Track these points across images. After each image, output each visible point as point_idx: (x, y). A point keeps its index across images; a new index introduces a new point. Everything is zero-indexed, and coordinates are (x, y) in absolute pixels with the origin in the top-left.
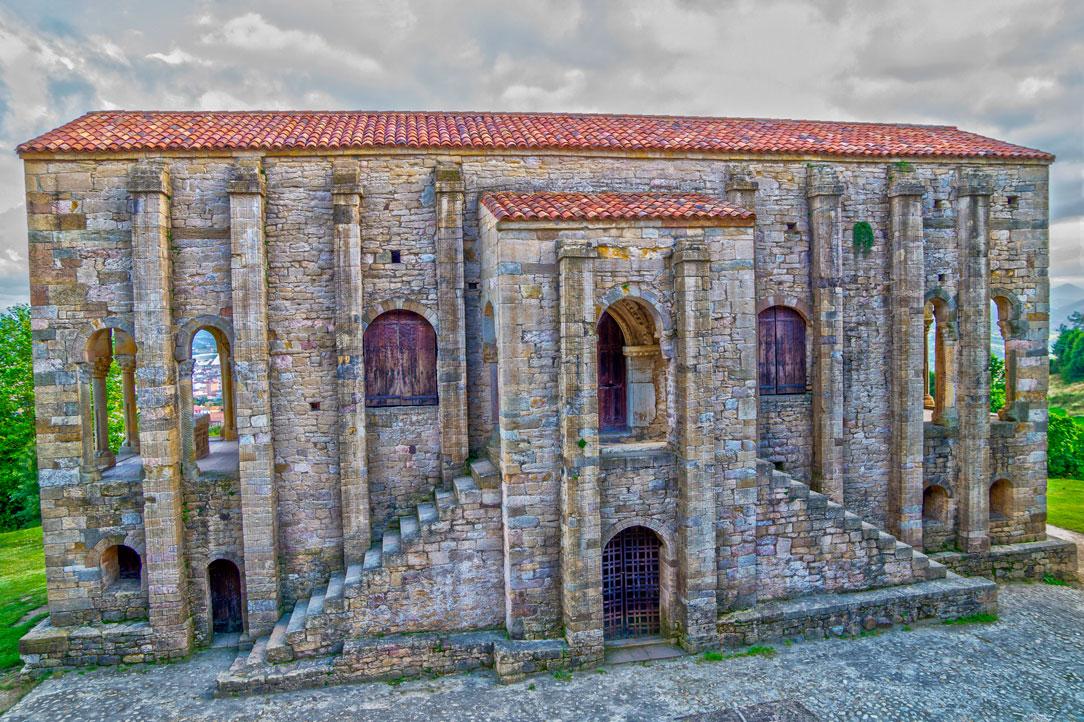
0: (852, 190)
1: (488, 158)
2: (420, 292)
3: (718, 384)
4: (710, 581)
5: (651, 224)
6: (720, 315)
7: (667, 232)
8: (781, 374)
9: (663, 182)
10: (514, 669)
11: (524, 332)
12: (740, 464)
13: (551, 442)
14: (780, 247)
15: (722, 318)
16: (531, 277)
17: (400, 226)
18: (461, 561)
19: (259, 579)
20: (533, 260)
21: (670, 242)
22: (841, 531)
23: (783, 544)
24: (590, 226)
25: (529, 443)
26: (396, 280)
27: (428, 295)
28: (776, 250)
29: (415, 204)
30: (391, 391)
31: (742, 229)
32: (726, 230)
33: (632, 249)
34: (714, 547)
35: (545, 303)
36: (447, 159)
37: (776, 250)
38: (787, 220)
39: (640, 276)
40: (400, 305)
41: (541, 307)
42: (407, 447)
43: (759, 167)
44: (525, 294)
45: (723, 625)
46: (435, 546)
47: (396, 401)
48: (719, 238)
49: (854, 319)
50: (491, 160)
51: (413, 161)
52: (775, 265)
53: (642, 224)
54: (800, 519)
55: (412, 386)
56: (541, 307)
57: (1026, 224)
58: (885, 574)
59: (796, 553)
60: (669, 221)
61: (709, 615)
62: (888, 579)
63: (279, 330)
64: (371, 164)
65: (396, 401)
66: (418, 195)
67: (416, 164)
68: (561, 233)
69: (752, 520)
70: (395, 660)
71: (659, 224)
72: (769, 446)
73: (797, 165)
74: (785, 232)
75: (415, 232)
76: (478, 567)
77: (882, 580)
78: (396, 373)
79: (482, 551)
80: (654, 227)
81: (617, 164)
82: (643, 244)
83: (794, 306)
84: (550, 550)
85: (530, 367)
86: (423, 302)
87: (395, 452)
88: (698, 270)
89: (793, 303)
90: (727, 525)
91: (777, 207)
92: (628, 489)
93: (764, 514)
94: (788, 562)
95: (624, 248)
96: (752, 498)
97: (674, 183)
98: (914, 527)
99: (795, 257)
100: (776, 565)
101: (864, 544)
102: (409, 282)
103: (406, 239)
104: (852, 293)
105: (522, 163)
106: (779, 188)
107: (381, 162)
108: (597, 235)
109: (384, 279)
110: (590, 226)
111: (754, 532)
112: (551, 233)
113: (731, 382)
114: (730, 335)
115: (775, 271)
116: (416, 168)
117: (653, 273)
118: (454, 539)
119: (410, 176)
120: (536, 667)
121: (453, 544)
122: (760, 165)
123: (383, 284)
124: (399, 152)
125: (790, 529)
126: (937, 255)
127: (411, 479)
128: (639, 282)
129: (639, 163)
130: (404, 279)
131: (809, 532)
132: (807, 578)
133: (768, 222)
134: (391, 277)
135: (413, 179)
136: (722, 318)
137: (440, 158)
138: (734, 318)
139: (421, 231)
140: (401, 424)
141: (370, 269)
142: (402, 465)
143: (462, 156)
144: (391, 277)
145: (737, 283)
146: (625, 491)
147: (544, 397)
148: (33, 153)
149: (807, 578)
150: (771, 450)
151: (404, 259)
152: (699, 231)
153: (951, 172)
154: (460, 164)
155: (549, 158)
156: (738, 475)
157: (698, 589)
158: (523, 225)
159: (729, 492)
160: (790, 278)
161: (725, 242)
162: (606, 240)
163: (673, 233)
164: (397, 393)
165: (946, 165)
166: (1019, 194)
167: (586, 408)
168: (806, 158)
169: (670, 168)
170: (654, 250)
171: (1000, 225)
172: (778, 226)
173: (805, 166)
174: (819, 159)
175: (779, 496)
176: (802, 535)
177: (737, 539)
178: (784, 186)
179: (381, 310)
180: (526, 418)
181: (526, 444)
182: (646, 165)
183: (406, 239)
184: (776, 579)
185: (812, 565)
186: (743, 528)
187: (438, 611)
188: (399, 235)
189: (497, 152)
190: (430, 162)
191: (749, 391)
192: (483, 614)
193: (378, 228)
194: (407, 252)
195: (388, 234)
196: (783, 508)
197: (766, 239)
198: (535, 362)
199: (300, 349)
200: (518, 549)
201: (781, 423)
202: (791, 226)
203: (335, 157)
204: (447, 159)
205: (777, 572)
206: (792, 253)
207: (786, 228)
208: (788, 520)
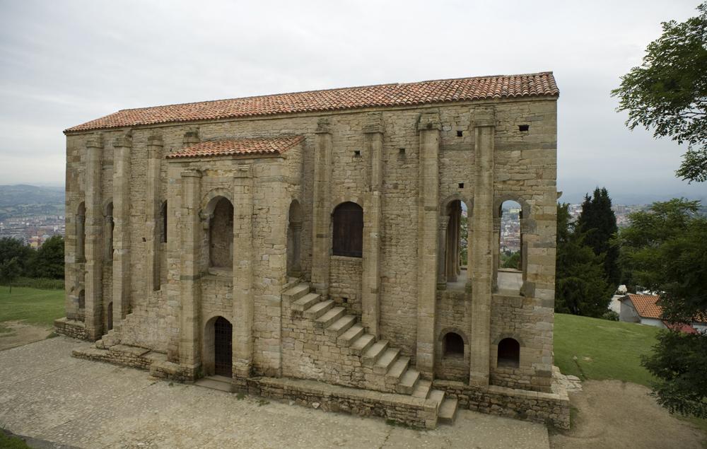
0: (396, 128)
6: (260, 208)
7: (235, 162)
9: (287, 131)
14: (350, 166)
15: (261, 209)
18: (161, 318)
19: (117, 311)
22: (335, 345)
23: (299, 345)
36: (193, 127)
43: (339, 118)
48: (261, 164)
49: (395, 212)
57: (535, 146)
58: (365, 380)
62: (366, 384)
63: (133, 205)
64: (167, 131)
68: (191, 164)
70: (126, 358)
71: (231, 158)
77: (363, 384)
81: (264, 123)
82: (224, 168)
88: (241, 182)
95: (216, 171)
97: (291, 131)
98: (426, 358)
101: (351, 357)
104: (394, 195)
106: (350, 130)
107: (170, 130)
108: (204, 165)
110: (202, 160)
120: (165, 376)
125: (302, 336)
126: (458, 170)
128: (222, 189)
129: (275, 121)
132: (314, 370)
136: (261, 209)
148: (67, 132)
149: (314, 370)
153: (472, 111)
154: (198, 128)
155: (234, 123)
162: (208, 167)
163: (239, 162)
165: (465, 106)
166: (528, 123)
169: (290, 123)
170: (230, 171)
171: (511, 147)
172: (348, 153)
174: (375, 110)
176: (309, 342)
182: (279, 122)
185: (316, 362)
191: (276, 251)
199: (139, 214)
202: (357, 153)
203: (155, 128)
204: (193, 127)
206: (356, 170)
207: (354, 153)
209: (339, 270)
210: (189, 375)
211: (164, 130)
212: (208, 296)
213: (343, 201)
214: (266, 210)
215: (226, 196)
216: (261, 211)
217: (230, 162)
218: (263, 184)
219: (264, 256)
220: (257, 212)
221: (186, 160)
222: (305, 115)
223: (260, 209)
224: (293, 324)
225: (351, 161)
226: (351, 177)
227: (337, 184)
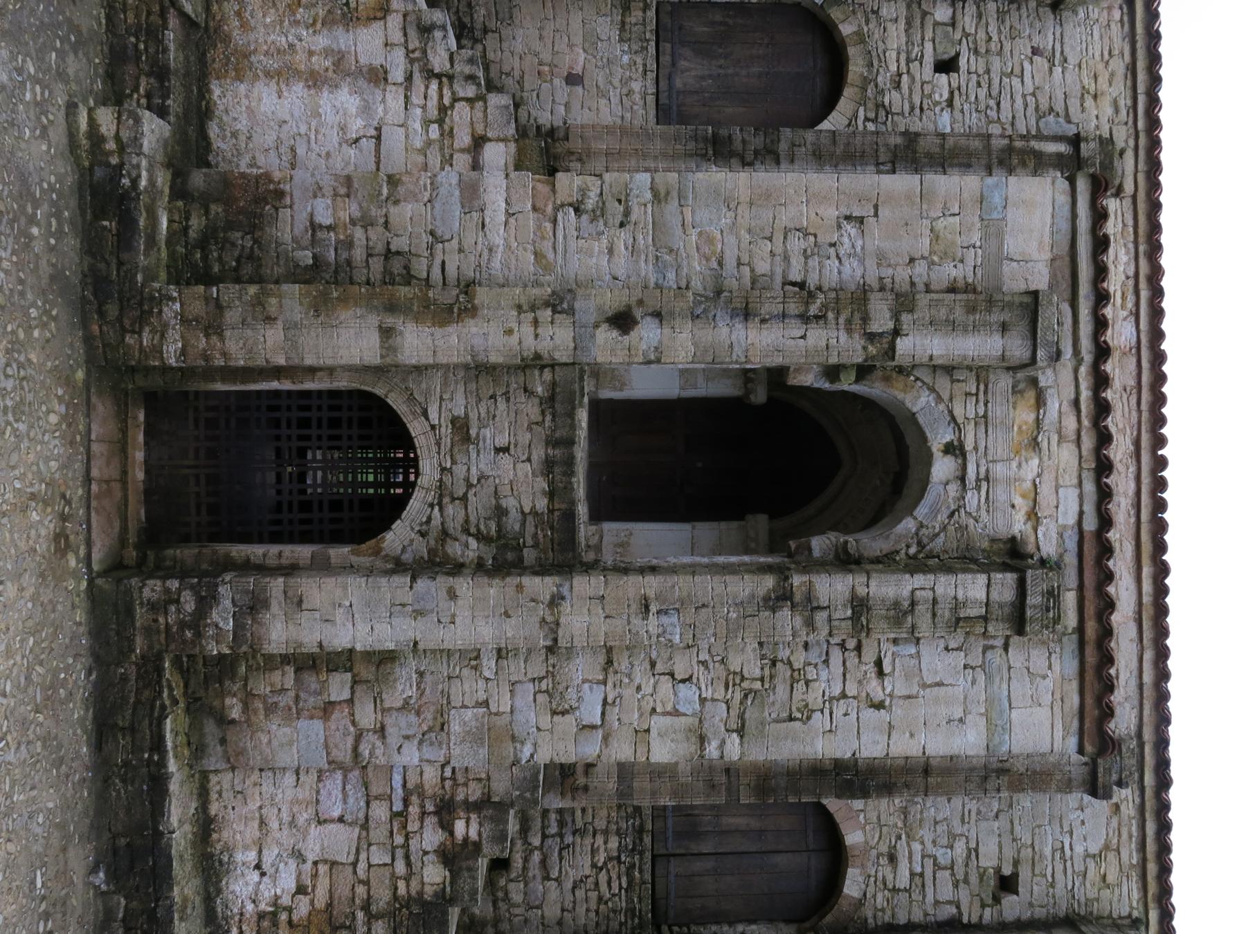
1: (1131, 246)
2: (879, 106)
3: (735, 666)
4: (274, 636)
5: (1089, 508)
6: (887, 669)
7: (1071, 545)
8: (698, 865)
10: (103, 139)
11: (861, 220)
12: (545, 721)
13: (621, 273)
14: (968, 857)
15: (881, 673)
16: (976, 238)
17: (1003, 74)
20: (1012, 245)
21: (1049, 548)
24: (1083, 370)
25: (622, 225)
26: (903, 63)
27: (875, 120)
28: (960, 847)
29: (1044, 106)
30: (687, 52)
31: (1076, 724)
32: (1075, 685)
33: (1036, 461)
34: (358, 647)
35: (920, 268)
36: (1128, 169)
37: (960, 847)
38: (1024, 874)
39: (978, 480)
40: (856, 68)
41: (912, 260)
42: (578, 69)
43: (1129, 810)
44: (940, 224)
45: (159, 671)
46: (397, 37)
47: (666, 59)
50: (1127, 253)
51: (1122, 103)
52: (929, 845)
53: (1090, 487)
54: (401, 885)
55: (696, 92)
56: (912, 260)
59: (315, 876)
60: (1096, 547)
61: (189, 634)
64: (1115, 28)
65: (666, 59)
66: (1062, 113)
67: (1117, 111)
68: (1066, 308)
69: (411, 755)
71: (1090, 524)
72: (544, 837)
73: (1136, 895)
74: (998, 870)
75: (992, 103)
76: (343, 128)
78: (722, 62)
79: (378, 138)
80: (1081, 513)
82: (1046, 490)
83: (846, 890)
84: (377, 265)
85: (786, 232)
86: (861, 110)
87: (571, 46)
88: (1001, 606)
89: (853, 885)
90: (403, 686)
91: (1048, 851)
92: (505, 450)
93: (420, 790)
94: (299, 856)
95: (1035, 444)
96: (466, 756)
99: (946, 892)
100: (293, 823)
102: (898, 86)
103: (979, 84)
105: (1125, 313)
106: (1087, 855)
108: (1062, 384)
109: (904, 40)
110: (1083, 370)
111: (382, 761)
112: (1065, 285)
113: (738, 696)
114: (844, 695)
115: (917, 847)
116: (1109, 111)
117: (983, 513)
118: (409, 78)
119: (1095, 97)
120: (103, 197)
121: (398, 75)
122: (1132, 812)
123: (896, 36)
124: (1142, 76)
127: (517, 73)
128: (962, 479)
130: (905, 78)
131: (366, 907)
132: (250, 907)
133: (1017, 828)
134: (908, 53)
135: (1089, 102)
136: (881, 673)
137: (1129, 155)
138: (879, 706)
139: (993, 114)
140: (626, 59)
141: (925, 14)
142: (546, 56)
143: (1134, 197)
144: (908, 53)
145: (958, 714)
146: (502, 441)
147: (720, 264)
149: (250, 907)
150: (536, 841)
151: (943, 78)
152: (1071, 620)
156: (519, 717)
157: (254, 606)
158: (1084, 223)
159: (482, 696)
160: (903, 880)
161: (1049, 683)
162: (1053, 406)
164: (683, 64)
167: (706, 335)
168: (1153, 916)
170: (1033, 516)
172: (1009, 853)
173: (1135, 914)
175: (459, 827)
176: (361, 890)
177: (367, 715)
178: (1091, 864)
179: (846, 29)
180: (675, 222)
181: (619, 218)
183: (979, 84)
184: (256, 824)
186: (390, 730)
187: (252, 37)
188: (988, 71)
189: (1143, 263)
190: (1122, 136)
192: (235, 135)
193: (1000, 32)
194: (955, 85)
195: (987, 51)
196: (432, 837)
197: (983, 824)
198: (796, 244)
200: (385, 191)
201: (594, 866)
202: (1007, 884)
205: (274, 825)
206: (956, 885)
207: (1007, 871)
208: (400, 853)
209: (606, 832)
210: (130, 340)
211: (1117, 14)
212: (502, 405)
213: (853, 838)
214: (878, 695)
215: (929, 498)
216: (872, 673)
217: (1071, 520)
218: (981, 678)
219: (688, 693)
220: (869, 655)
221: (1085, 288)
222: (1148, 677)
223: (879, 663)
224: (423, 814)
225: (984, 863)
226: (929, 863)
227: (905, 812)
